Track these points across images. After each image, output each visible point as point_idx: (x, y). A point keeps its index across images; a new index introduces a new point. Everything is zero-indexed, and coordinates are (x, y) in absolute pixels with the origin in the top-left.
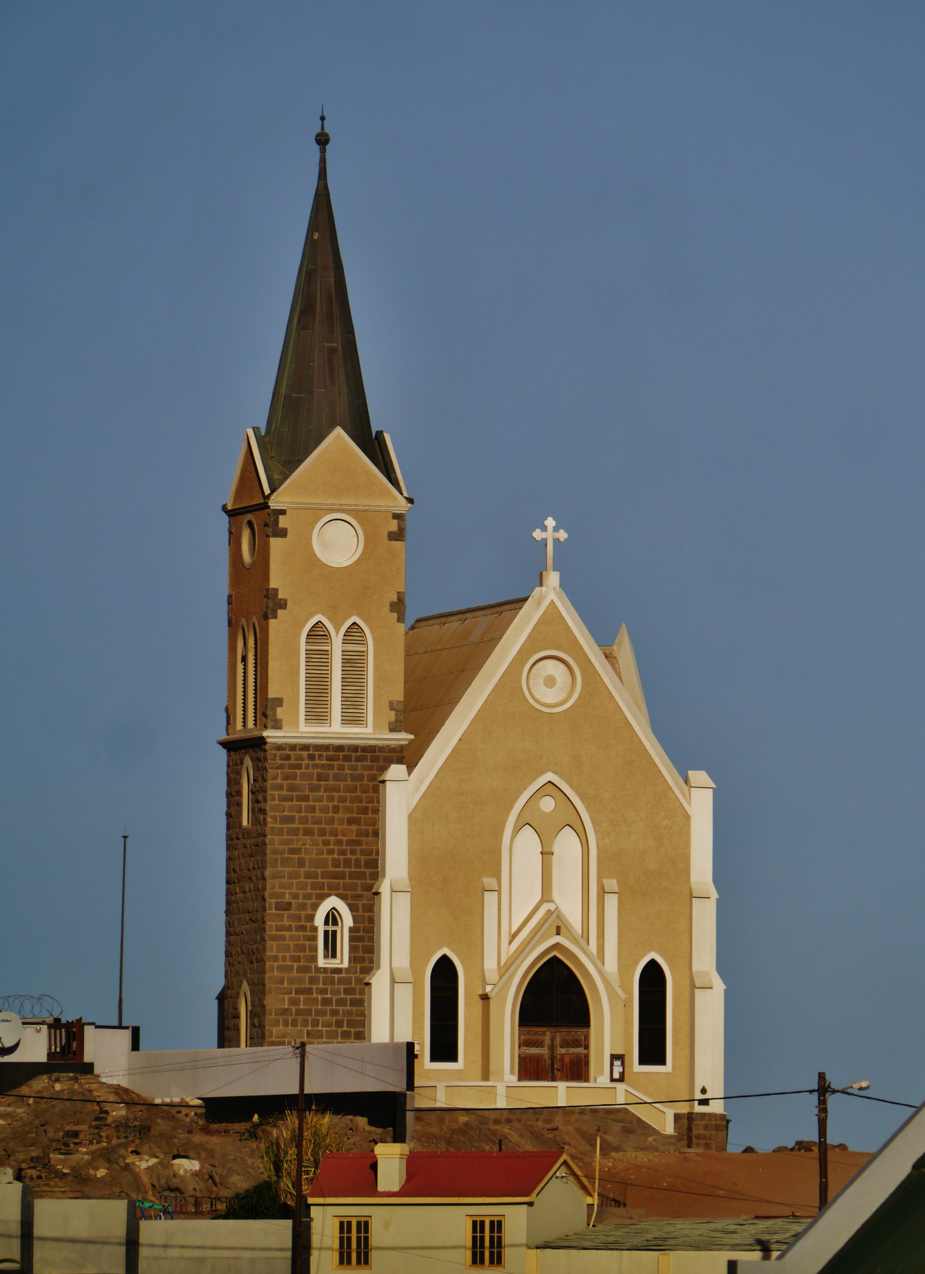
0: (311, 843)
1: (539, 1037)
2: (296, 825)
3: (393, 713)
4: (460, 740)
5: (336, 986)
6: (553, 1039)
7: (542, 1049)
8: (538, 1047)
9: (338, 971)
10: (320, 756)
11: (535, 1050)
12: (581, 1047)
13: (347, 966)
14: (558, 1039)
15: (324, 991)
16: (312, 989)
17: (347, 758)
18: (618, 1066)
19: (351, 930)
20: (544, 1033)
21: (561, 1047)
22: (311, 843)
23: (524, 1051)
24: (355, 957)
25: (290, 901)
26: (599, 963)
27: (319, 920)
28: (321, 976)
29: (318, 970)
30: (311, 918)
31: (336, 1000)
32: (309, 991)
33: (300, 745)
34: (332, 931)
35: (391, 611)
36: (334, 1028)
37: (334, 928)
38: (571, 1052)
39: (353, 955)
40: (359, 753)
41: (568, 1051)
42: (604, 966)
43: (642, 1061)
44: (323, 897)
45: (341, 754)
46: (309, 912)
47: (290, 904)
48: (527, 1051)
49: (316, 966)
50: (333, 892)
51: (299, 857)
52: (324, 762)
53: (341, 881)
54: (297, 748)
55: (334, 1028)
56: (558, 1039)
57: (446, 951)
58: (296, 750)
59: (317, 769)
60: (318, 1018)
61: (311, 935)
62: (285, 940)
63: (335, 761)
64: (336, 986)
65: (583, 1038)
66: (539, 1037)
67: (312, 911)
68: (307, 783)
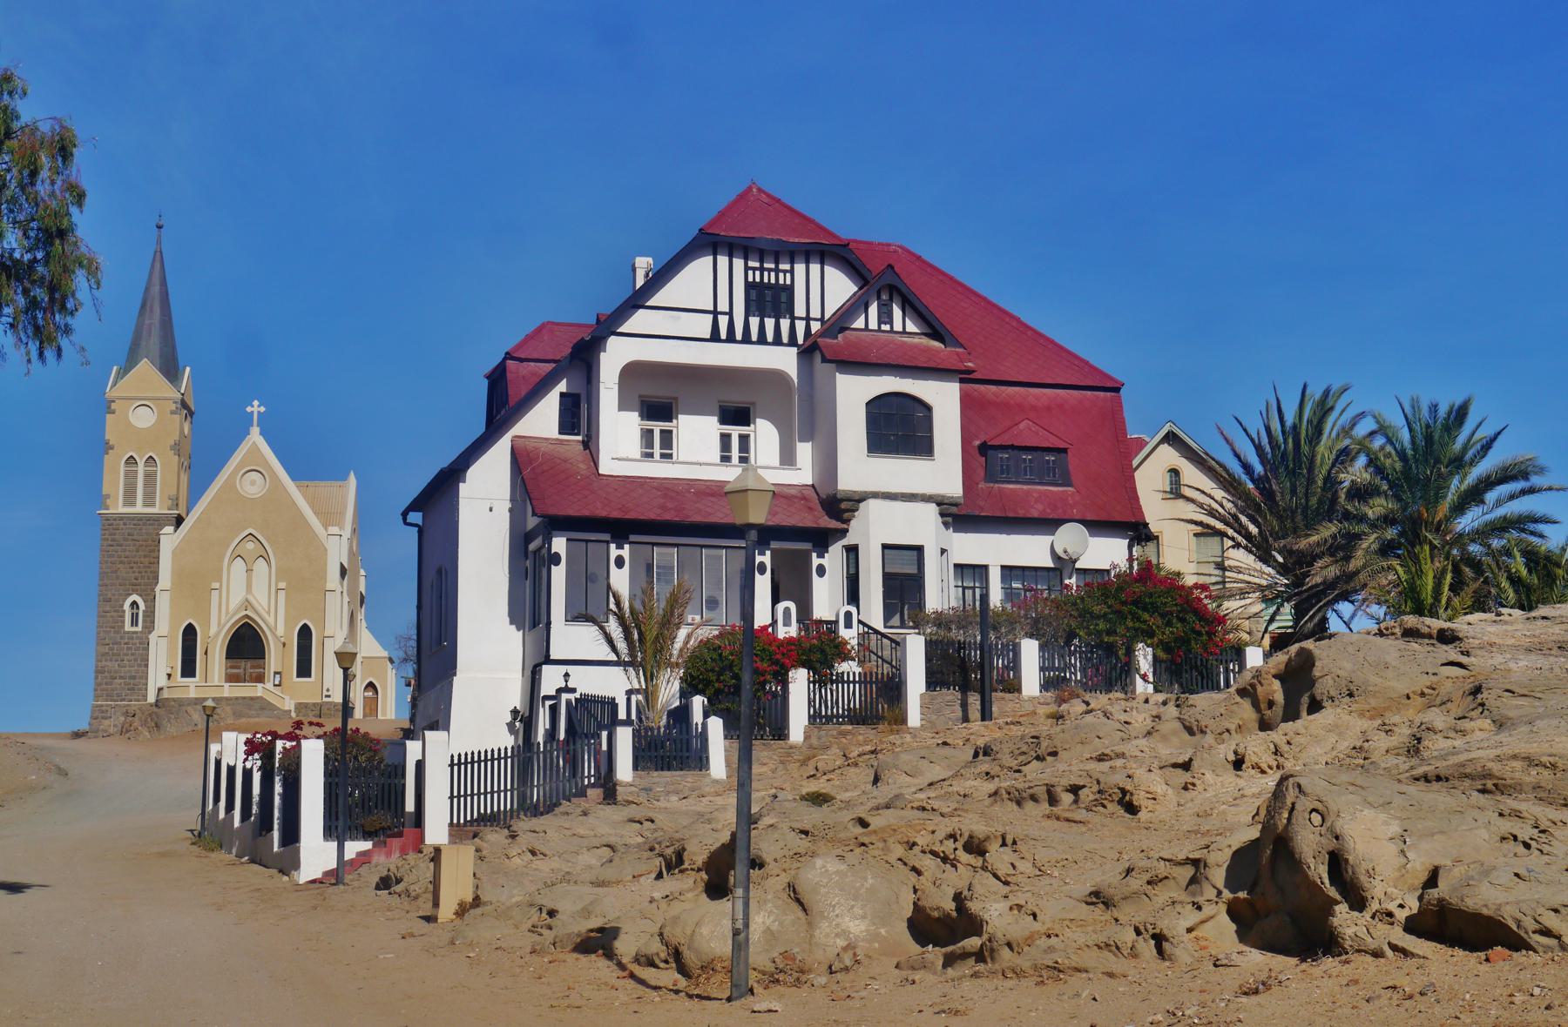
9: (136, 633)
15: (126, 644)
29: (125, 632)
30: (122, 606)
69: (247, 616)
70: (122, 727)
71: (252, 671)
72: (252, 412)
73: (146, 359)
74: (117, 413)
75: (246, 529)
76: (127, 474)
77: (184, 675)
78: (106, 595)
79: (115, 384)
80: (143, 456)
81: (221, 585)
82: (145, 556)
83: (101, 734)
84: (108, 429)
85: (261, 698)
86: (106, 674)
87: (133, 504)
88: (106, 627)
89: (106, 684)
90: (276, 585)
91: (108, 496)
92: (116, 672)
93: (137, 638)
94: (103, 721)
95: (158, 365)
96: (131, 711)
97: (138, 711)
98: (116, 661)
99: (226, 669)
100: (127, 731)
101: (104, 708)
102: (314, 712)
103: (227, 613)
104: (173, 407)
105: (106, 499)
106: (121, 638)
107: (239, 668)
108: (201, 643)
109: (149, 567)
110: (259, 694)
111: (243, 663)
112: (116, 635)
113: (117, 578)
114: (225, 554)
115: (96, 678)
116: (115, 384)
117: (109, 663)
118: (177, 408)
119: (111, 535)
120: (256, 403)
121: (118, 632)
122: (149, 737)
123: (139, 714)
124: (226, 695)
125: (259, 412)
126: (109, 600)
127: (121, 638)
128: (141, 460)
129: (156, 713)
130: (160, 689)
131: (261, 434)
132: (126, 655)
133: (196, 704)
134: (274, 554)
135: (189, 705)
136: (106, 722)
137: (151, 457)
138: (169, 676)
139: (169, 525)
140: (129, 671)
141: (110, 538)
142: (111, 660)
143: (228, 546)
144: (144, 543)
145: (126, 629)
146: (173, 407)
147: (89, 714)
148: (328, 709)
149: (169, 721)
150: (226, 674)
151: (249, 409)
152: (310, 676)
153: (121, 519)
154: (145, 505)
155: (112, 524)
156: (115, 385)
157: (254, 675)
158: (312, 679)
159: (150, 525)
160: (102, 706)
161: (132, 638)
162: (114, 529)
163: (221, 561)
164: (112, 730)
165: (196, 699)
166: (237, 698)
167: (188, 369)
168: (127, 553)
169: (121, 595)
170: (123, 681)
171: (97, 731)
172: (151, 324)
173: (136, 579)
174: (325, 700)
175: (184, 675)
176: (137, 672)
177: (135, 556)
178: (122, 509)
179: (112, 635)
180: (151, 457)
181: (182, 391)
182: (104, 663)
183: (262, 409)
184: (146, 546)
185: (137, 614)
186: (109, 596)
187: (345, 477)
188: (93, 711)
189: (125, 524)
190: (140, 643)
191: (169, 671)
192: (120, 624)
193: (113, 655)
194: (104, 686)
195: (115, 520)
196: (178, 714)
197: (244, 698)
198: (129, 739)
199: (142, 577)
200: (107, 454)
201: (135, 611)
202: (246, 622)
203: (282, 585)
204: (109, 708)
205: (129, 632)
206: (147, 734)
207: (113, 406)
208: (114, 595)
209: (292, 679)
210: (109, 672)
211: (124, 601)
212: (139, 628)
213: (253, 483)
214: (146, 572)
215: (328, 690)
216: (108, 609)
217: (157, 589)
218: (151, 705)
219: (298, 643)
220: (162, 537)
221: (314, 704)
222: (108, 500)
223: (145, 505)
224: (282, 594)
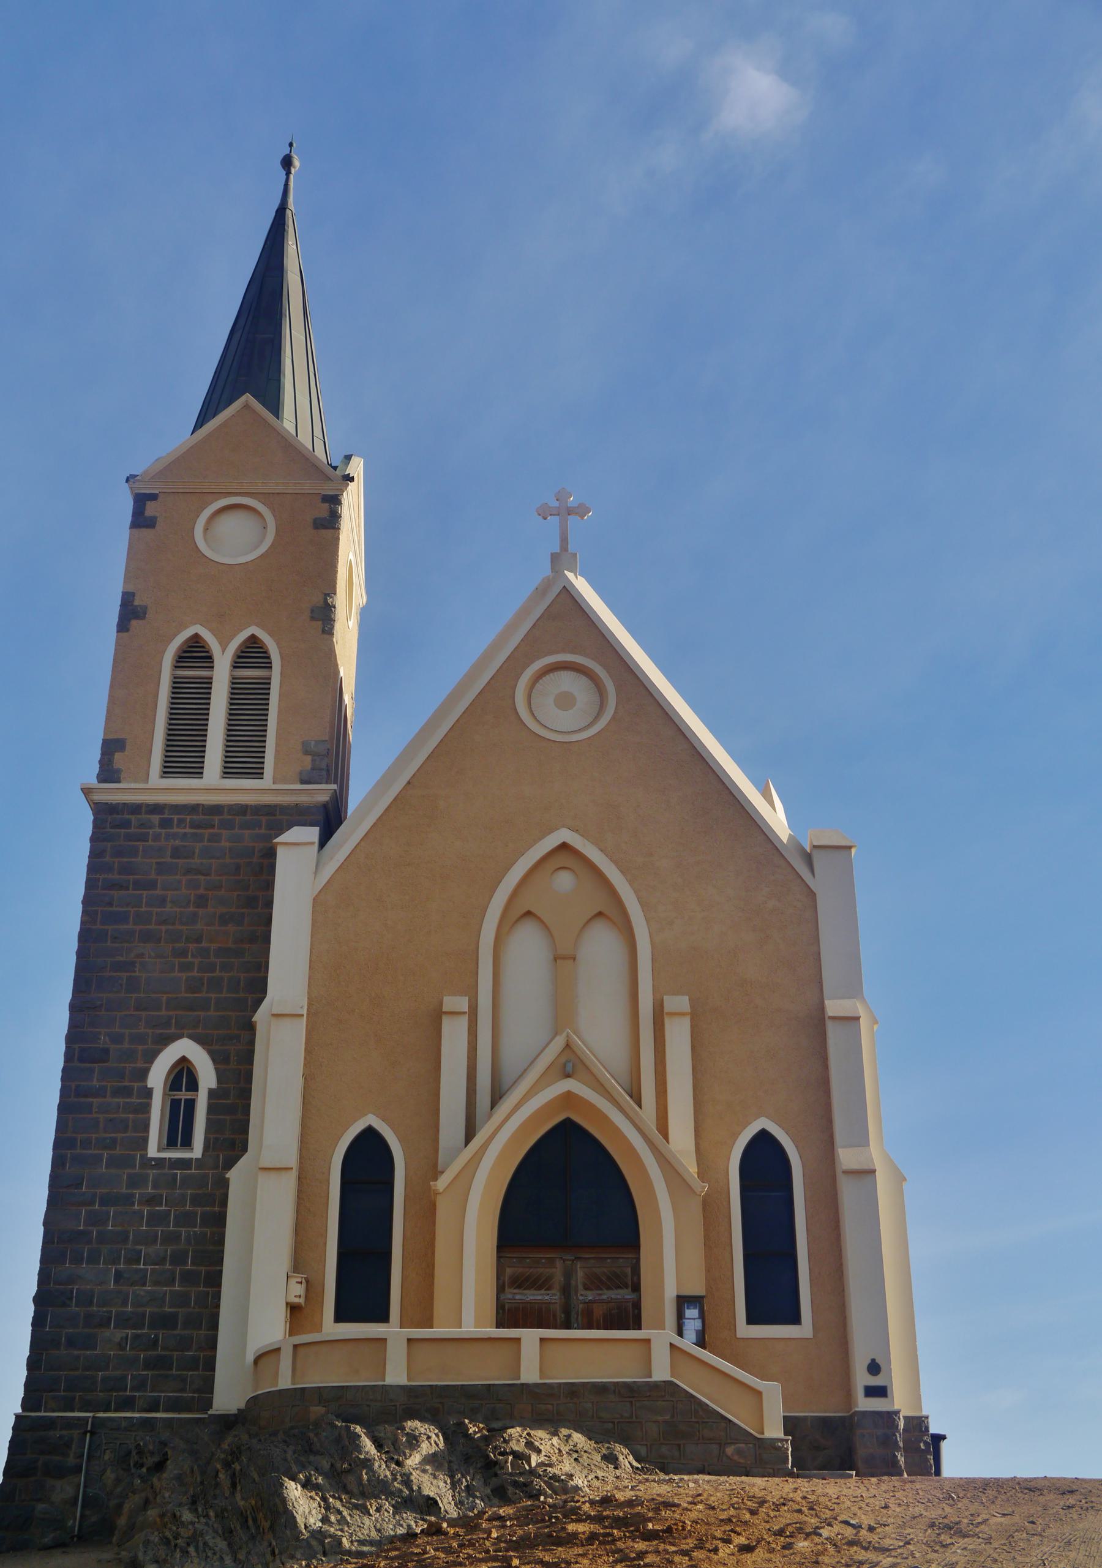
0: (153, 954)
1: (541, 1270)
2: (130, 926)
3: (309, 758)
4: (409, 783)
5: (178, 1191)
6: (568, 1274)
7: (548, 1292)
8: (540, 1288)
9: (185, 1164)
10: (180, 821)
11: (534, 1295)
12: (627, 1287)
13: (200, 1156)
14: (580, 1274)
15: (152, 1200)
16: (133, 1195)
17: (227, 825)
18: (694, 1319)
19: (211, 1093)
20: (551, 1261)
21: (586, 1288)
22: (153, 954)
23: (510, 1296)
24: (217, 1139)
25: (106, 1046)
26: (658, 1138)
27: (157, 1076)
28: (151, 1173)
29: (147, 1162)
30: (144, 1074)
31: (175, 1217)
32: (128, 1199)
33: (148, 805)
34: (186, 1100)
35: (313, 618)
36: (168, 1267)
37: (189, 1095)
38: (604, 1297)
39: (212, 1136)
40: (248, 817)
41: (601, 1295)
42: (668, 1142)
43: (751, 1320)
44: (166, 1041)
45: (217, 818)
46: (140, 1065)
47: (106, 1051)
48: (518, 1297)
49: (144, 1156)
50: (186, 1032)
51: (130, 976)
52: (188, 830)
53: (202, 1014)
54: (143, 811)
55: (168, 1267)
56: (580, 1274)
57: (371, 1120)
58: (140, 813)
59: (175, 840)
60: (138, 1247)
61: (141, 1103)
62: (91, 1113)
63: (206, 828)
64: (178, 1191)
65: (629, 1271)
66: (541, 1270)
67: (145, 1063)
68: (154, 861)
71: (590, 1296)
74: (158, 527)
75: (551, 830)
76: (177, 685)
87: (196, 770)
99: (500, 1289)
134: (645, 905)
145: (153, 1151)
150: (500, 1306)
157: (598, 1312)
160: (51, 1423)
162: (129, 837)
174: (865, 1404)
185: (191, 1105)
186: (103, 1041)
205: (160, 1162)
212: (197, 1150)
215: (874, 1368)
217: (260, 1017)
220: (281, 853)
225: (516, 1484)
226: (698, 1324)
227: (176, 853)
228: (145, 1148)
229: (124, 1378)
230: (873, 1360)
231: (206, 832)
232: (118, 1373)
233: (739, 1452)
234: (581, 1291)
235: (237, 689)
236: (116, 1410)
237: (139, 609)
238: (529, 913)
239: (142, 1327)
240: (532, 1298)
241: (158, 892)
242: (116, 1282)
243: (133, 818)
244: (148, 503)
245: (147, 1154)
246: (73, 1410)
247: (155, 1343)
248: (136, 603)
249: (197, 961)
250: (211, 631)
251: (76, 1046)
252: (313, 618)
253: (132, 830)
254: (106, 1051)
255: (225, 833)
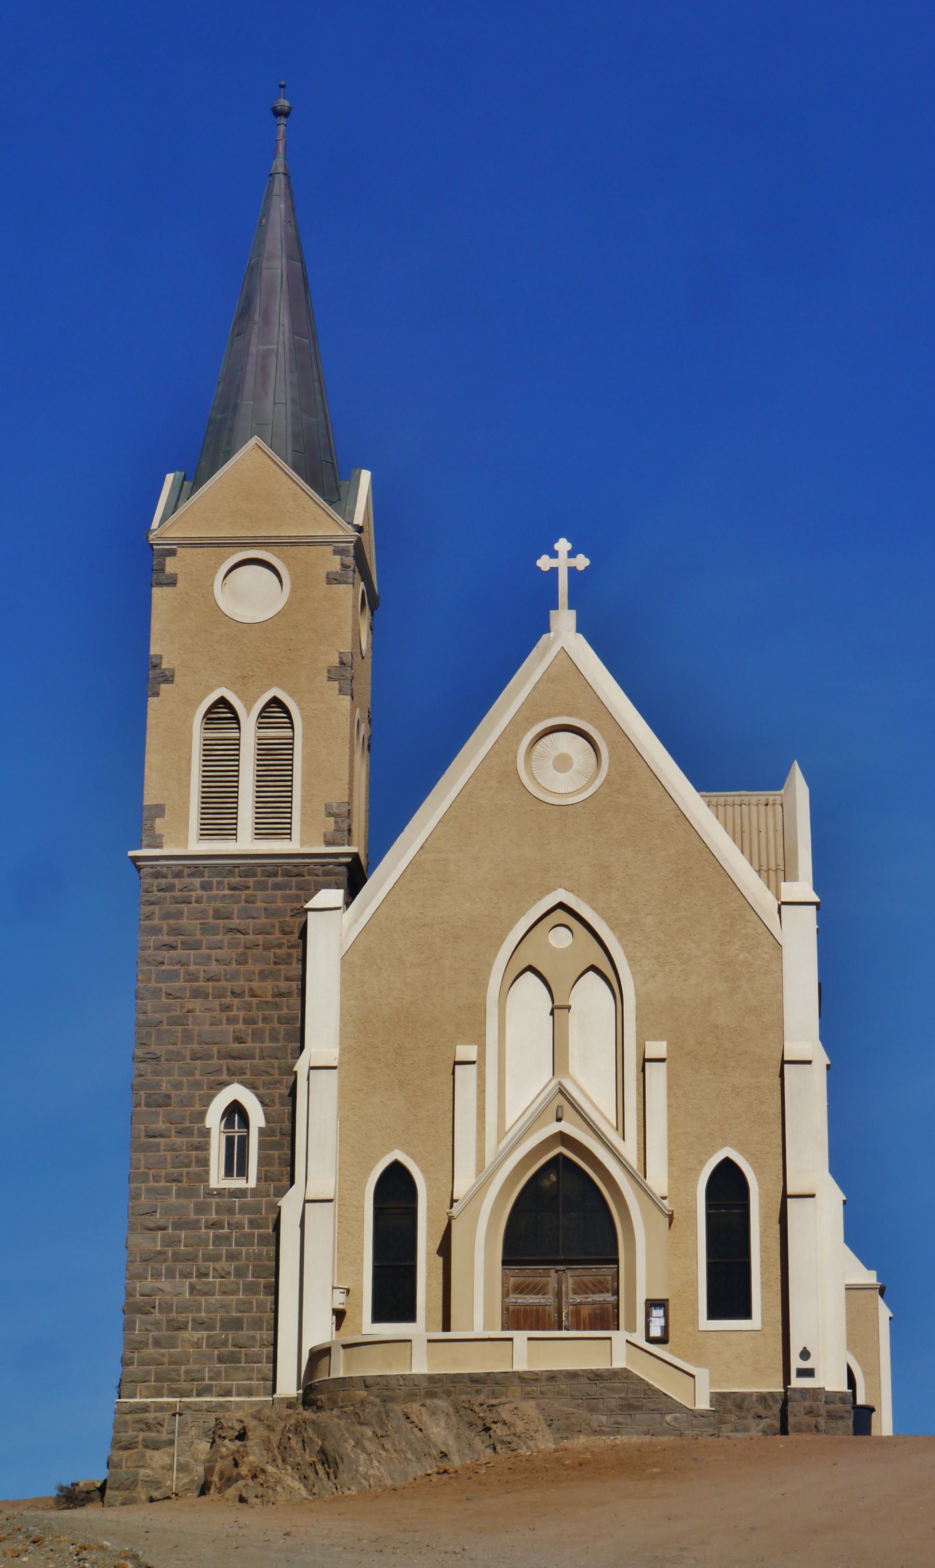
4: (422, 847)
8: (537, 1293)
11: (532, 1299)
12: (608, 1291)
16: (199, 1221)
17: (263, 886)
18: (660, 1317)
19: (261, 1131)
21: (575, 1292)
23: (514, 1300)
28: (214, 1201)
29: (210, 1193)
30: (202, 1116)
35: (330, 679)
38: (590, 1300)
46: (198, 1108)
47: (169, 1097)
48: (519, 1301)
50: (236, 1078)
52: (227, 892)
55: (232, 1279)
69: (563, 1138)
70: (209, 1471)
72: (554, 571)
73: (255, 440)
75: (549, 890)
76: (209, 748)
77: (379, 1316)
78: (158, 1085)
79: (173, 507)
80: (255, 700)
81: (482, 1054)
82: (263, 976)
83: (142, 1493)
84: (156, 626)
85: (625, 1374)
86: (157, 1315)
87: (230, 832)
88: (156, 1178)
89: (157, 1343)
90: (641, 1049)
91: (160, 810)
92: (183, 1309)
93: (242, 1210)
94: (149, 1453)
95: (290, 459)
96: (232, 1421)
97: (251, 1423)
98: (187, 1276)
99: (505, 1294)
100: (228, 1481)
101: (150, 1416)
102: (764, 1423)
103: (501, 1132)
104: (334, 563)
105: (153, 819)
106: (200, 1209)
107: (540, 1290)
108: (430, 1220)
109: (277, 1006)
110: (619, 1363)
111: (551, 1277)
112: (184, 1201)
113: (188, 1037)
114: (490, 966)
115: (129, 1326)
116: (173, 507)
117: (164, 1284)
118: (344, 566)
119: (167, 916)
120: (563, 546)
121: (189, 1193)
122: (304, 1493)
123: (256, 1432)
124: (521, 1365)
125: (572, 571)
126: (166, 1101)
127: (200, 1209)
128: (249, 711)
129: (313, 1422)
130: (320, 1355)
131: (579, 630)
132: (217, 1258)
133: (431, 1394)
134: (631, 959)
135: (411, 1396)
136: (159, 1458)
137: (275, 701)
138: (340, 1315)
139: (328, 886)
140: (225, 1307)
141: (164, 925)
142: (170, 1274)
143: (501, 940)
144: (260, 939)
146: (334, 563)
147: (109, 1435)
148: (810, 1412)
149: (358, 1443)
150: (505, 1309)
151: (544, 563)
152: (746, 1313)
153: (196, 872)
154: (261, 833)
155: (170, 888)
156: (176, 508)
157: (585, 1311)
158: (755, 1323)
159: (277, 887)
160: (145, 1408)
161: (230, 1210)
163: (481, 985)
164: (175, 1481)
165: (431, 1379)
166: (552, 1376)
167: (366, 476)
168: (214, 967)
169: (197, 1085)
170: (205, 1333)
171: (131, 1485)
172: (265, 356)
173: (239, 1040)
174: (797, 1383)
175: (379, 1316)
176: (244, 1306)
177: (235, 976)
178: (197, 846)
179: (173, 1199)
180: (275, 701)
181: (359, 519)
182: (149, 1283)
183: (582, 562)
184: (267, 948)
185: (244, 1141)
187: (777, 781)
188: (119, 1426)
189: (205, 887)
190: (252, 1223)
191: (339, 1300)
192: (194, 1169)
193: (177, 1257)
194: (151, 1351)
195: (178, 875)
196: (382, 1425)
197: (573, 1375)
198: (242, 1500)
199: (258, 1036)
200: (157, 694)
201: (237, 1132)
202: (561, 1154)
203: (656, 1048)
204: (167, 1415)
205: (220, 1193)
206: (296, 1485)
207: (171, 565)
208: (177, 1086)
209: (695, 1321)
210: (166, 1308)
211: (207, 1100)
212: (252, 1182)
213: (563, 763)
214: (265, 1019)
215: (805, 1355)
216: (161, 1126)
217: (301, 1066)
218: (290, 1404)
219: (709, 1217)
221: (763, 1398)
222: (158, 821)
223: (261, 833)
224: (657, 1075)
225: (502, 1442)
226: (662, 1322)
227: (218, 915)
228: (207, 1181)
229: (201, 1371)
230: (805, 1348)
231: (244, 894)
232: (197, 1367)
233: (675, 1419)
234: (571, 1295)
235: (265, 751)
236: (198, 1395)
237: (167, 672)
238: (530, 969)
239: (215, 1329)
240: (531, 1301)
241: (204, 951)
242: (191, 1293)
243: (176, 881)
244: (168, 559)
245: (209, 1185)
246: (162, 1396)
247: (224, 1343)
248: (164, 666)
249: (242, 1014)
250: (235, 692)
251: (142, 1093)
252: (330, 679)
253: (177, 893)
254: (169, 1097)
255: (260, 894)
